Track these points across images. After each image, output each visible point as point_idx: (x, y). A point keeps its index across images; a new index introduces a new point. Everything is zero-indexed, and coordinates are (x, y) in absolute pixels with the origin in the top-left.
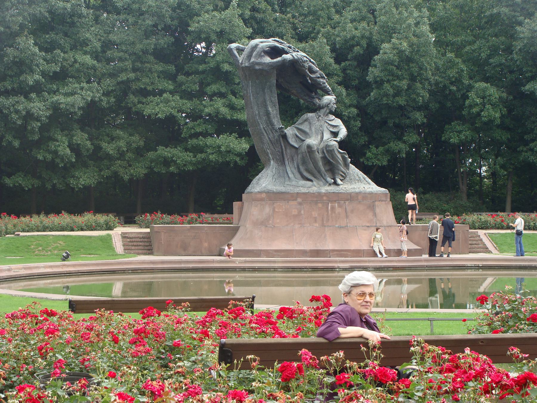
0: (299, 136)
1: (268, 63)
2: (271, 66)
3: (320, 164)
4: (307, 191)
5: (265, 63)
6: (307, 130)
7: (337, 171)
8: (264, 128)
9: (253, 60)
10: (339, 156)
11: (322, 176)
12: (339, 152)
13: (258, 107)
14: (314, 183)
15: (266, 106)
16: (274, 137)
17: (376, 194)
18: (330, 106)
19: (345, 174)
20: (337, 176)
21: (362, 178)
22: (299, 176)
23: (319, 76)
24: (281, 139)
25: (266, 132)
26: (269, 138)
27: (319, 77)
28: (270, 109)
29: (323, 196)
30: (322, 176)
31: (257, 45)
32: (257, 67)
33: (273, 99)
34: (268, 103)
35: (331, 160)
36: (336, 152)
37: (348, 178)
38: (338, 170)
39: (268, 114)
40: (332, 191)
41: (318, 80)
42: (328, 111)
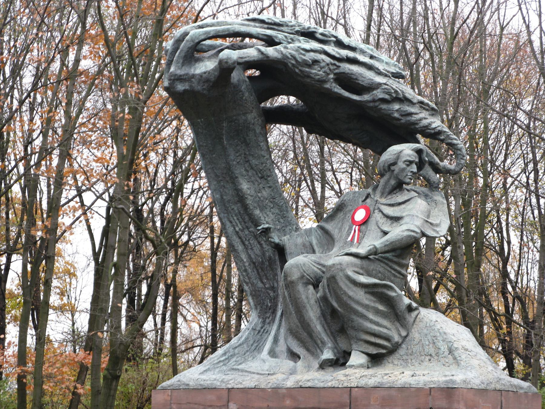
0: (316, 248)
1: (201, 75)
2: (207, 81)
3: (313, 314)
4: (252, 385)
5: (193, 76)
6: (335, 232)
7: (351, 332)
8: (237, 233)
9: (172, 69)
10: (360, 295)
11: (319, 347)
12: (355, 283)
13: (219, 182)
14: (300, 363)
15: (234, 180)
16: (264, 254)
17: (419, 389)
18: (396, 168)
19: (388, 339)
20: (354, 346)
21: (444, 348)
22: (282, 347)
23: (381, 96)
24: (277, 257)
25: (243, 243)
26: (249, 257)
27: (383, 101)
28: (245, 186)
29: (284, 396)
30: (319, 347)
31: (186, 34)
32: (180, 87)
33: (254, 162)
34: (239, 171)
35: (335, 304)
36: (343, 284)
37: (402, 351)
38: (353, 328)
39: (241, 198)
40: (309, 384)
41: (384, 106)
42: (393, 182)
